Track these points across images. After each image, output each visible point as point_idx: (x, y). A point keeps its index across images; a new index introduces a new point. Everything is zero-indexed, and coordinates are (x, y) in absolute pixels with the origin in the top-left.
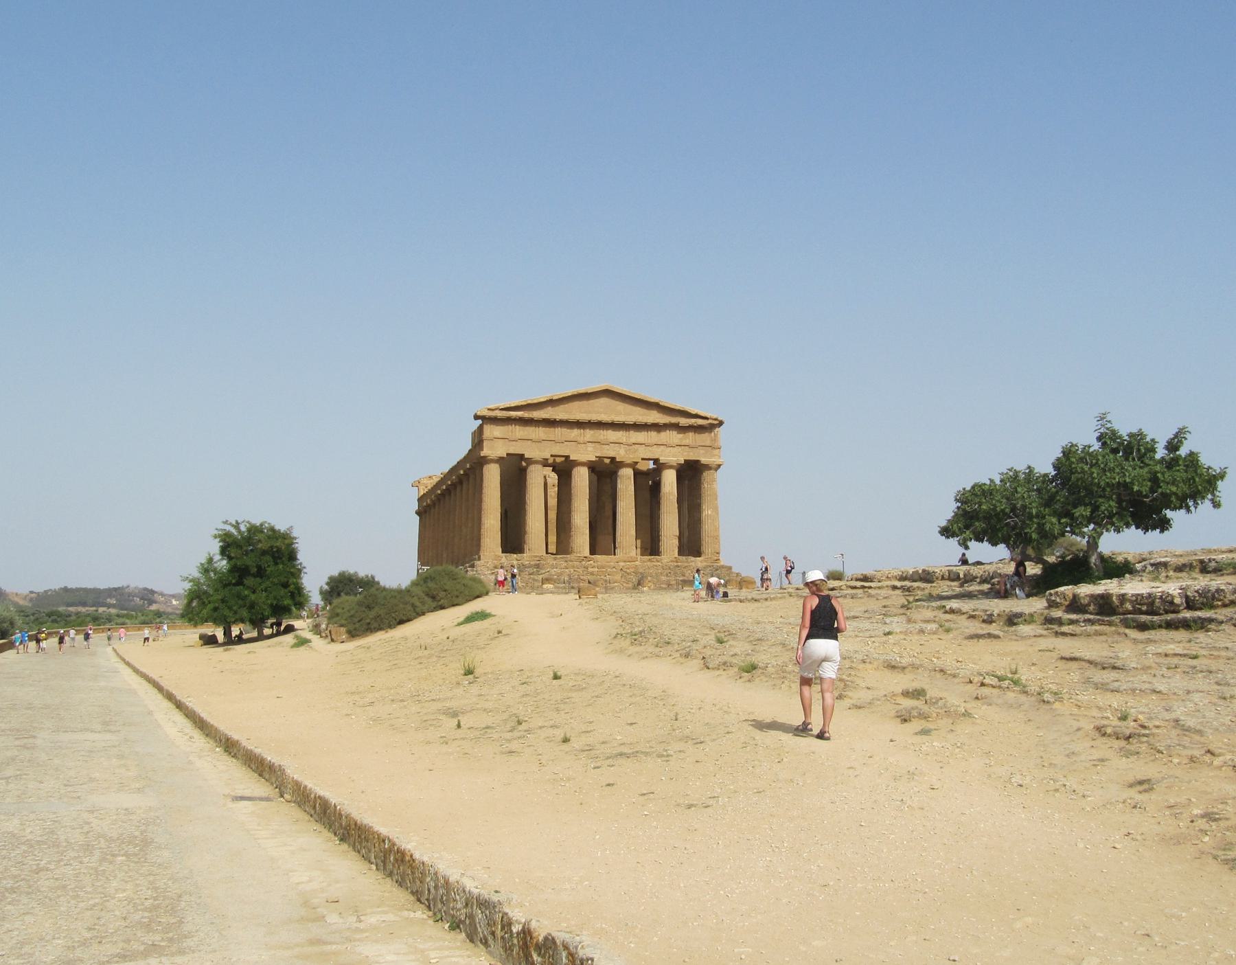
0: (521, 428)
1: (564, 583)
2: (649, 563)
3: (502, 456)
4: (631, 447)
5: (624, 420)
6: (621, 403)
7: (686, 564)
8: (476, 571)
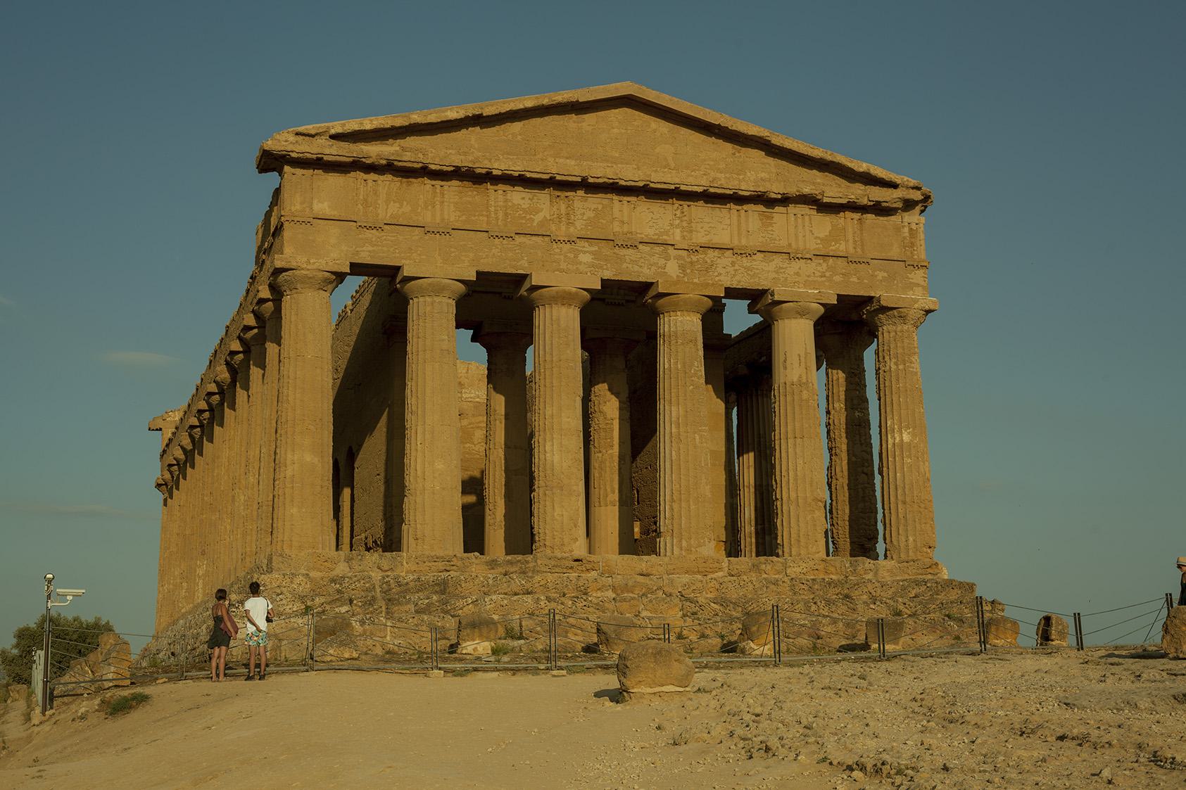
4: (694, 259)
5: (677, 180)
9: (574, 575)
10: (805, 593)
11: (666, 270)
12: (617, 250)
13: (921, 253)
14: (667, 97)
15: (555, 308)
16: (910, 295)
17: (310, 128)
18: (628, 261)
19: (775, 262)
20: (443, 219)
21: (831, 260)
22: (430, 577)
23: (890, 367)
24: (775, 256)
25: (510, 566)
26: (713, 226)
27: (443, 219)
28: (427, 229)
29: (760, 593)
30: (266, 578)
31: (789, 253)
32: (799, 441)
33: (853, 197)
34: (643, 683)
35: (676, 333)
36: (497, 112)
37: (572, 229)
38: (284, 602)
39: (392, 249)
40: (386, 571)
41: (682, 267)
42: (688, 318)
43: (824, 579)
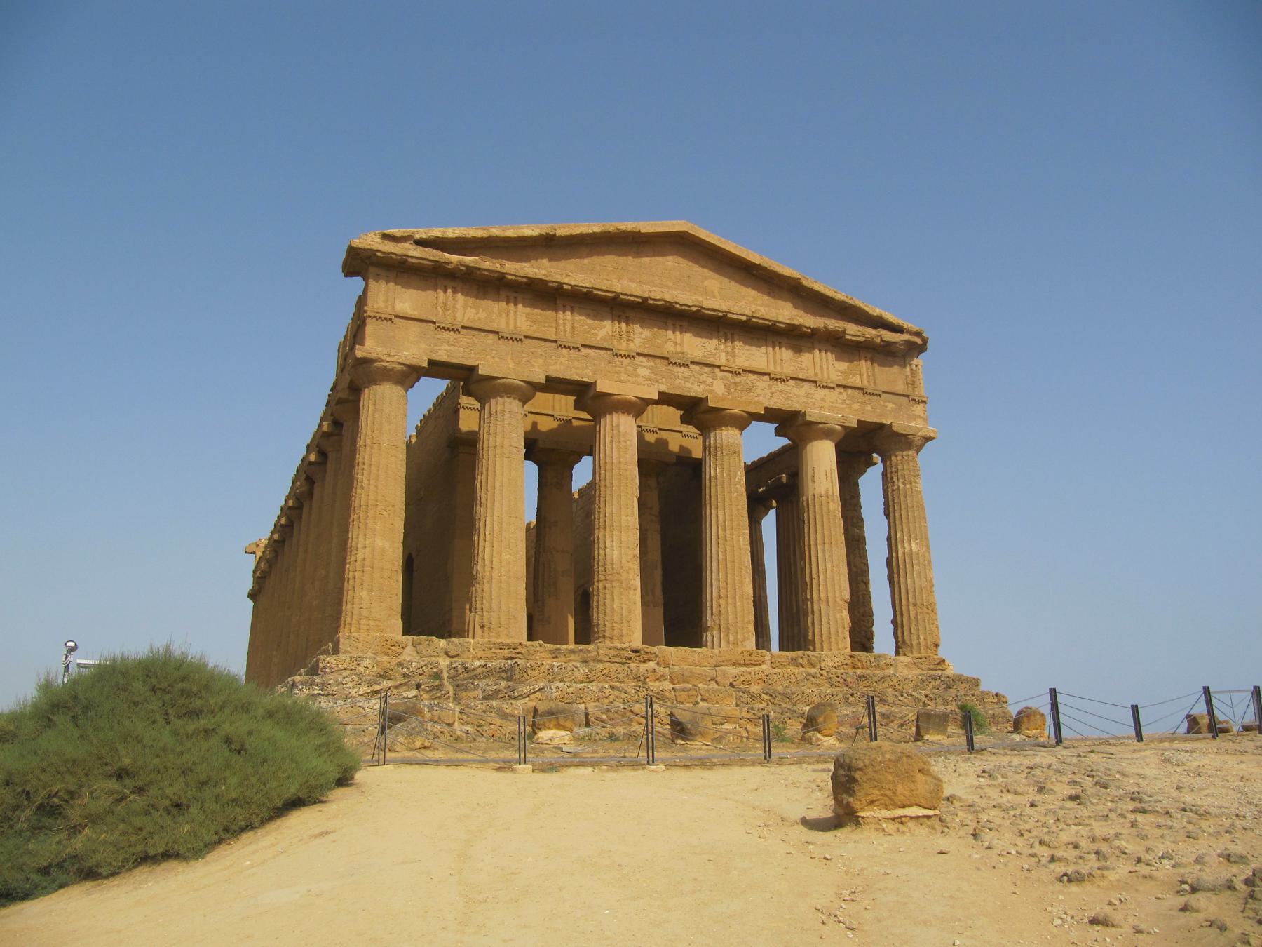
0: (471, 300)
1: (587, 725)
2: (791, 669)
3: (414, 362)
4: (737, 379)
5: (724, 308)
6: (717, 276)
7: (880, 674)
8: (322, 686)
9: (633, 665)
10: (840, 685)
11: (713, 388)
12: (671, 367)
13: (922, 391)
14: (717, 237)
15: (615, 416)
16: (913, 424)
17: (397, 232)
18: (680, 377)
19: (804, 388)
20: (516, 327)
21: (850, 391)
22: (496, 664)
23: (899, 487)
24: (804, 383)
25: (572, 655)
26: (752, 353)
27: (516, 327)
28: (501, 334)
29: (802, 684)
30: (332, 660)
31: (816, 382)
32: (827, 546)
33: (869, 336)
34: (877, 803)
35: (721, 445)
36: (568, 234)
37: (632, 346)
38: (350, 685)
39: (467, 350)
40: (452, 657)
42: (732, 432)
43: (855, 673)
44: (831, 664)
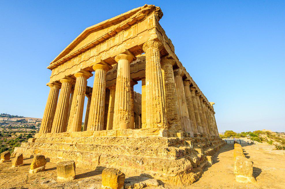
21: (127, 41)
41: (96, 60)
44: (110, 134)
